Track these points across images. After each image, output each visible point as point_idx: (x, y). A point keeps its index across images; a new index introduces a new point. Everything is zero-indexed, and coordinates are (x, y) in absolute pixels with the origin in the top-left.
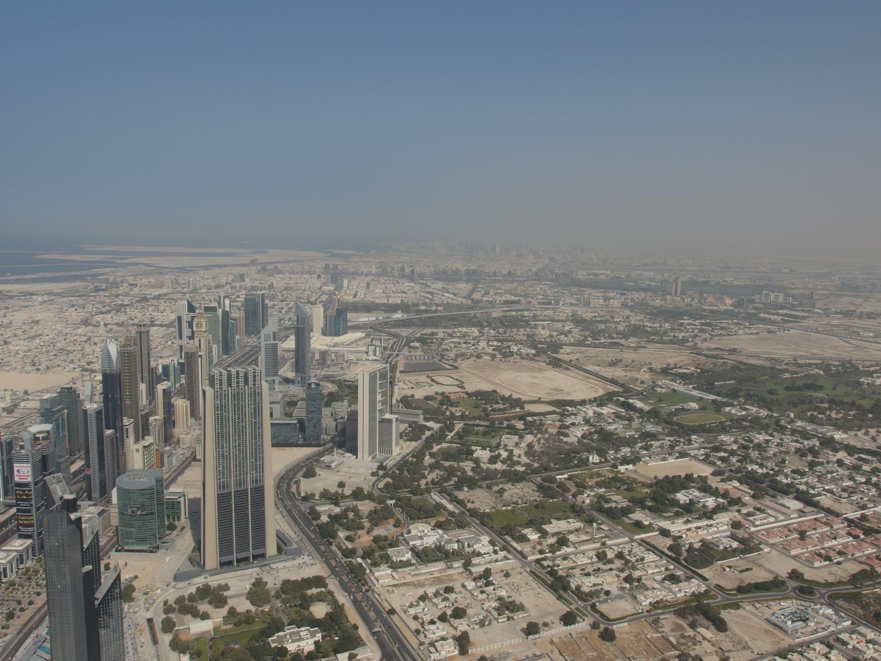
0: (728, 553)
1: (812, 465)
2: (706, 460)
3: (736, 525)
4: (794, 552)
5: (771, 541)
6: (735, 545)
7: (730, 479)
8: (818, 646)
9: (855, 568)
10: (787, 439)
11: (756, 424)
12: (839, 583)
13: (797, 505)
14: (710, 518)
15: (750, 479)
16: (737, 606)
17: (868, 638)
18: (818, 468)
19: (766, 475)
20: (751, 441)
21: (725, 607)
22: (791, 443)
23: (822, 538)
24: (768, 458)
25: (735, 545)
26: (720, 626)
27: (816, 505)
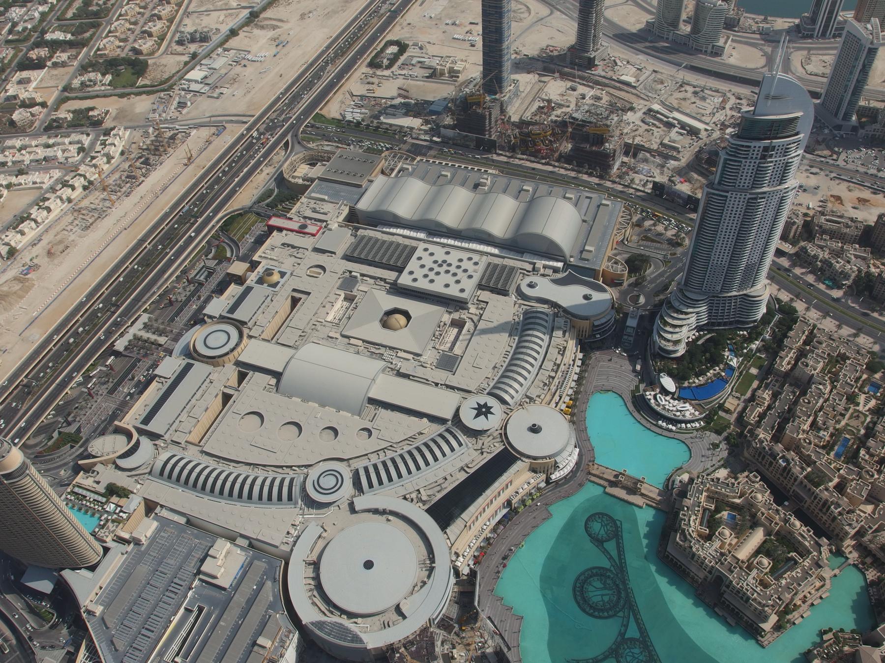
17: (18, 147)
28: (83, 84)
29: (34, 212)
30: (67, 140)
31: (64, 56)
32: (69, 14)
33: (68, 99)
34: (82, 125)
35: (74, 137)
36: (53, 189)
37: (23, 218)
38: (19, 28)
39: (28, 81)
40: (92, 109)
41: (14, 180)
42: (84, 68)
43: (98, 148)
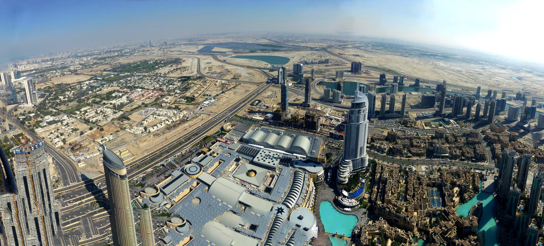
0: (127, 104)
1: (142, 81)
2: (118, 86)
3: (128, 97)
4: (142, 99)
5: (136, 99)
6: (128, 102)
7: (124, 88)
8: (151, 116)
9: (154, 99)
10: (136, 78)
11: (128, 76)
12: (153, 102)
13: (141, 90)
14: (121, 98)
15: (129, 87)
16: (131, 114)
18: (143, 82)
19: (132, 86)
20: (127, 80)
21: (129, 115)
22: (136, 78)
23: (147, 95)
24: (132, 82)
25: (128, 102)
26: (128, 119)
27: (144, 89)
28: (179, 101)
29: (158, 125)
30: (171, 111)
31: (177, 95)
32: (181, 88)
33: (175, 103)
34: (176, 109)
35: (173, 111)
36: (164, 121)
37: (156, 125)
38: (170, 89)
39: (168, 98)
40: (179, 106)
41: (157, 117)
42: (181, 98)
43: (178, 114)
